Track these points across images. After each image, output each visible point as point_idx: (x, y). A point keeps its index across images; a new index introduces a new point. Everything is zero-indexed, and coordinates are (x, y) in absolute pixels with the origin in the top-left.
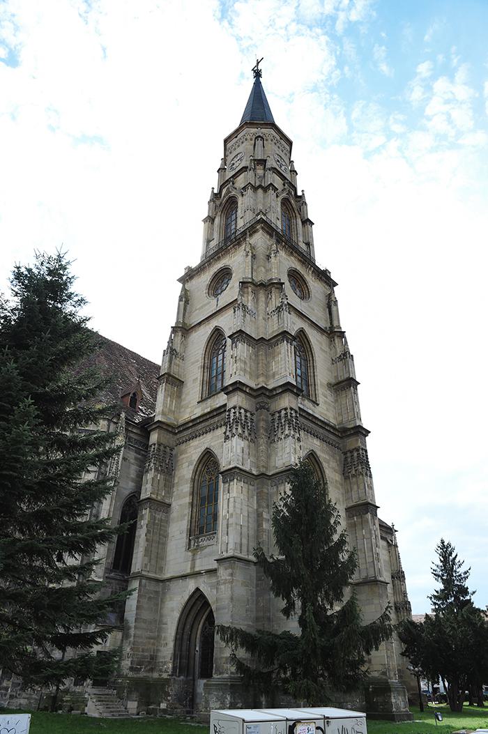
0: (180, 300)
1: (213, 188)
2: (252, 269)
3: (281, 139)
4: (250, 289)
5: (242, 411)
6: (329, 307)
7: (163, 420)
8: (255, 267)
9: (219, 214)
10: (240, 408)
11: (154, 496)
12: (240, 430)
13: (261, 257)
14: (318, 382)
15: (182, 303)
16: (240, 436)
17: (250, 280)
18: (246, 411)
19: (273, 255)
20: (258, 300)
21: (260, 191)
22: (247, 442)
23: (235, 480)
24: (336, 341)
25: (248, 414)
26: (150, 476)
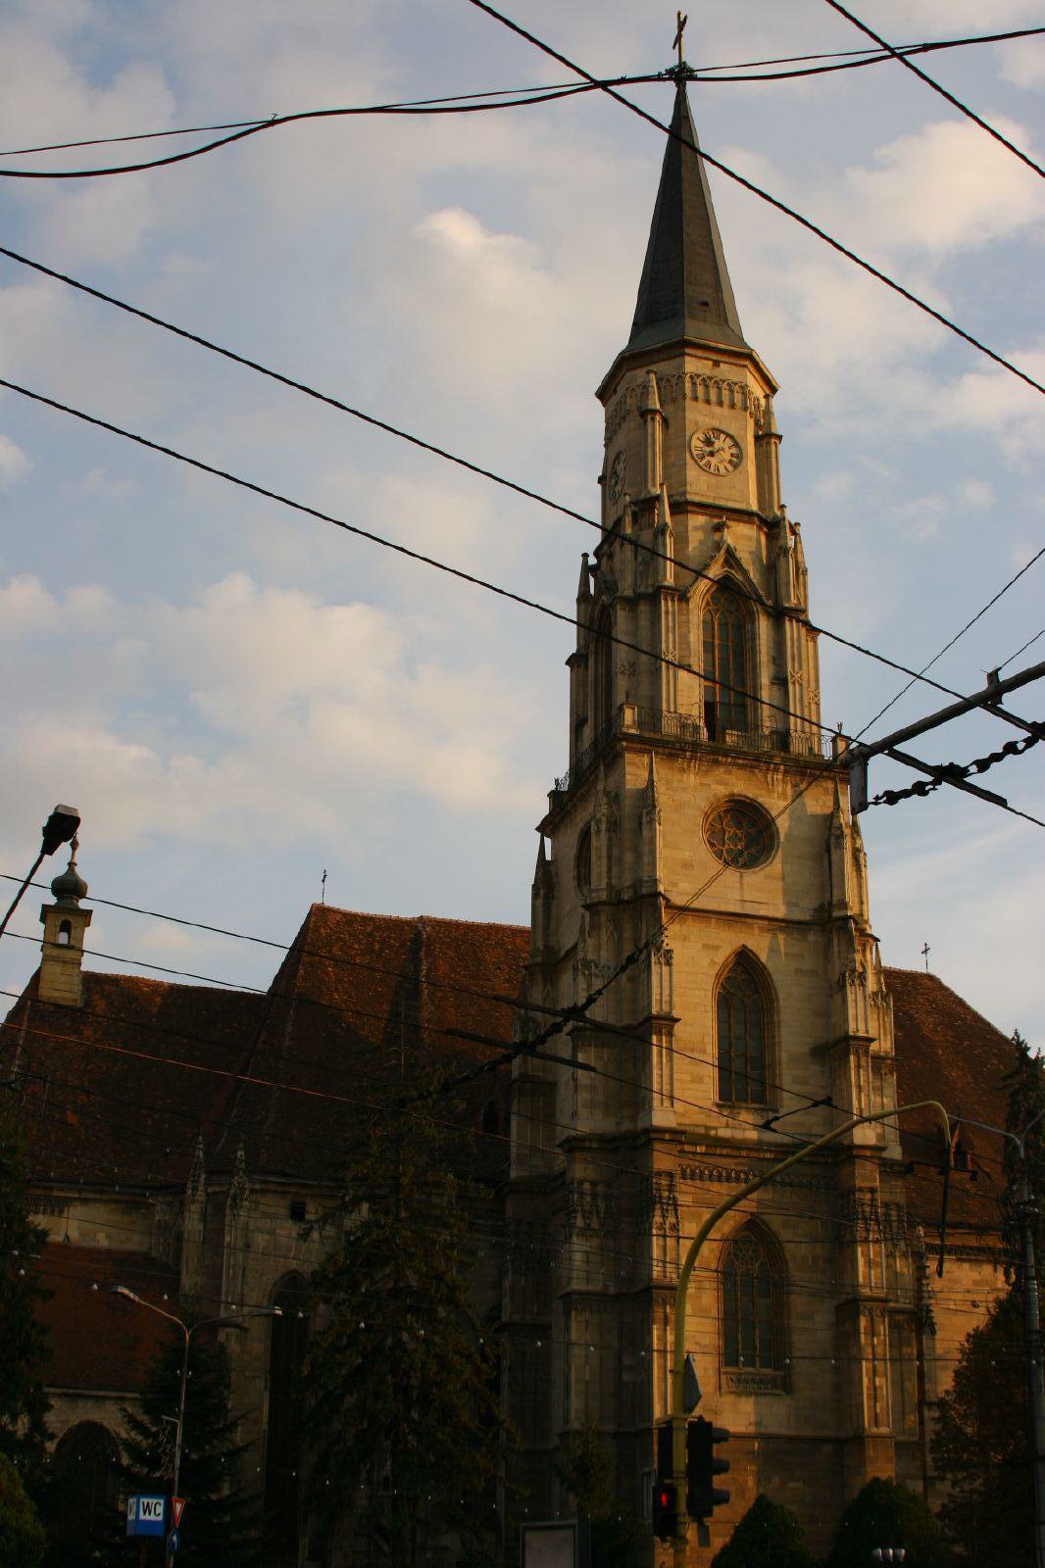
0: (535, 896)
1: (585, 556)
2: (609, 858)
3: (716, 364)
4: (603, 919)
5: (587, 1186)
6: (828, 850)
7: (522, 1174)
8: (615, 853)
9: (592, 647)
10: (581, 1183)
11: (517, 1318)
12: (579, 1222)
13: (628, 825)
14: (784, 1056)
15: (540, 902)
16: (581, 1233)
17: (604, 896)
18: (594, 1184)
19: (644, 820)
20: (620, 937)
21: (644, 608)
22: (595, 1242)
23: (573, 1314)
24: (835, 942)
25: (600, 1188)
26: (507, 1283)
